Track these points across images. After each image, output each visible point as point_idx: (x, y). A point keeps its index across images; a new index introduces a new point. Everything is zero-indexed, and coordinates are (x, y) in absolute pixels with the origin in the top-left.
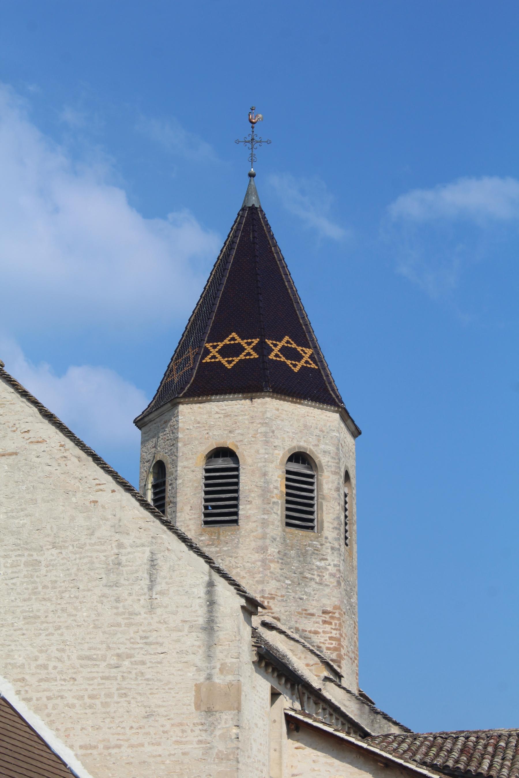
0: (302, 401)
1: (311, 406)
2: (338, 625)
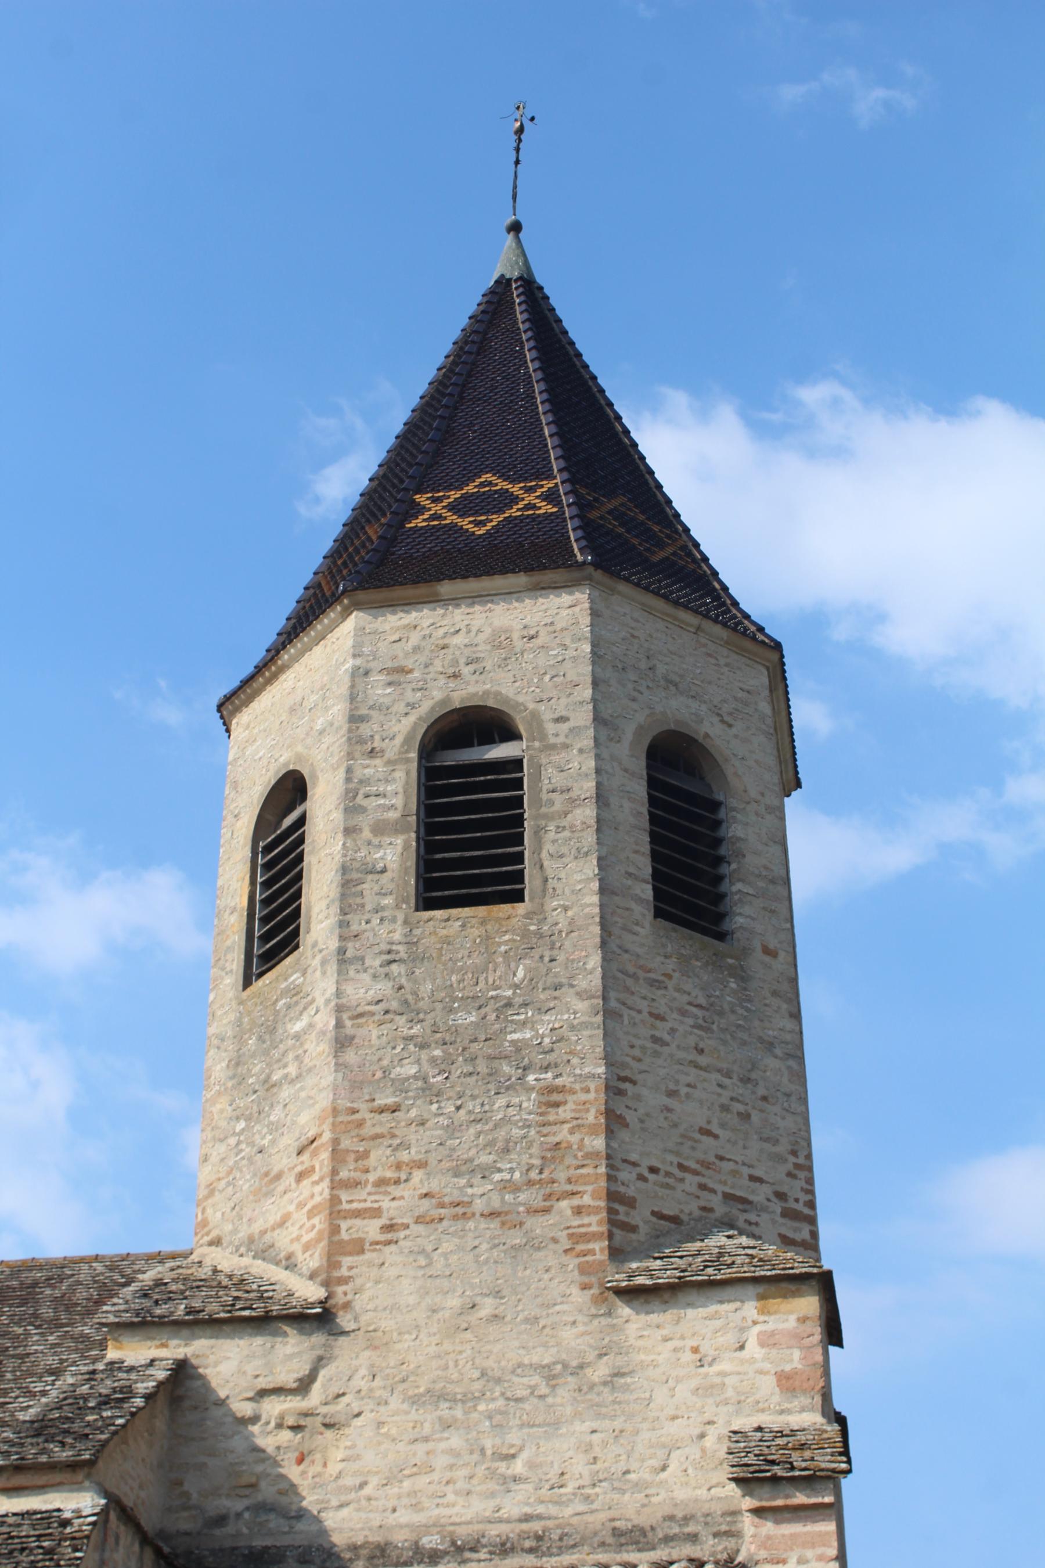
0: (280, 662)
1: (302, 653)
2: (326, 1162)
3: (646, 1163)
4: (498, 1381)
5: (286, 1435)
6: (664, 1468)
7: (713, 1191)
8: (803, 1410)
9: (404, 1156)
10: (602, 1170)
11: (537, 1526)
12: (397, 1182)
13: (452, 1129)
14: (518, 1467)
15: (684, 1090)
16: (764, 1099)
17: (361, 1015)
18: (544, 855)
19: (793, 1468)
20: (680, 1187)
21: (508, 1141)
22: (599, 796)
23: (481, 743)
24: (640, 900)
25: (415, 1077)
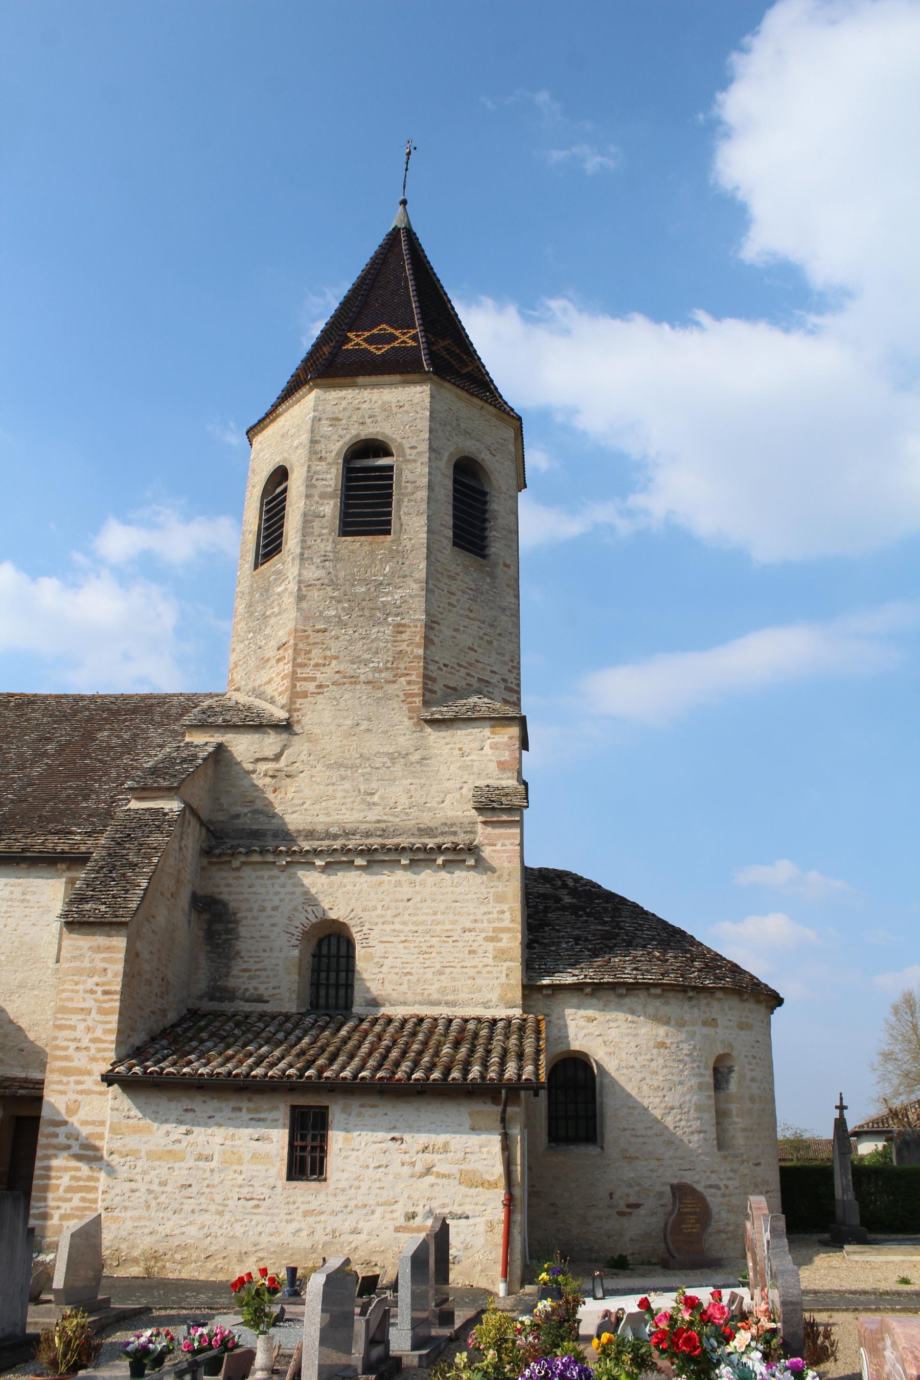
1: (289, 408)
3: (442, 662)
4: (368, 759)
5: (268, 780)
6: (443, 802)
7: (473, 677)
8: (508, 779)
9: (328, 653)
10: (422, 664)
11: (383, 825)
12: (324, 665)
13: (351, 642)
14: (376, 798)
15: (462, 629)
16: (500, 635)
17: (310, 585)
18: (402, 513)
19: (502, 804)
20: (458, 674)
21: (377, 649)
22: (429, 486)
23: (374, 457)
24: (446, 537)
25: (335, 616)
